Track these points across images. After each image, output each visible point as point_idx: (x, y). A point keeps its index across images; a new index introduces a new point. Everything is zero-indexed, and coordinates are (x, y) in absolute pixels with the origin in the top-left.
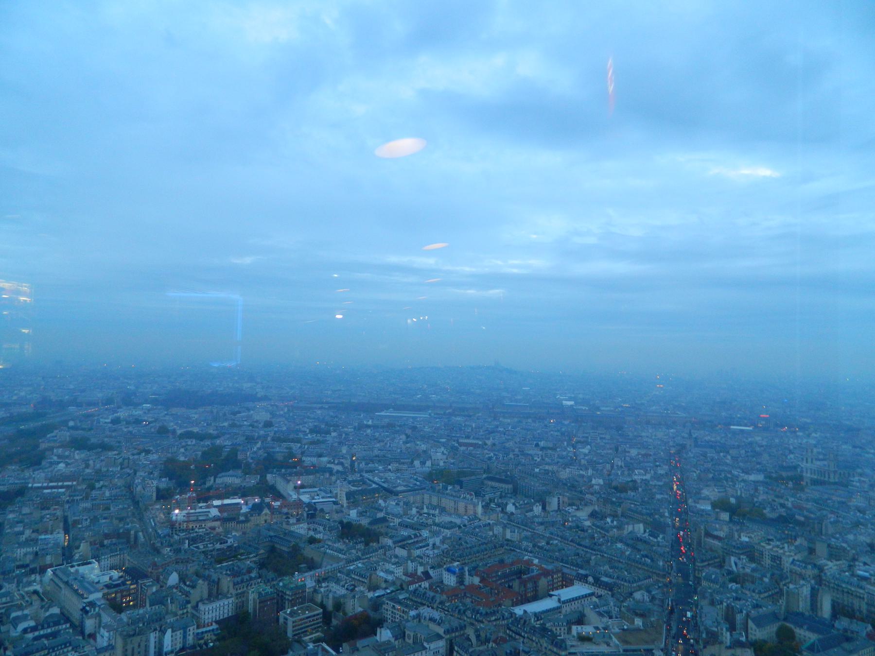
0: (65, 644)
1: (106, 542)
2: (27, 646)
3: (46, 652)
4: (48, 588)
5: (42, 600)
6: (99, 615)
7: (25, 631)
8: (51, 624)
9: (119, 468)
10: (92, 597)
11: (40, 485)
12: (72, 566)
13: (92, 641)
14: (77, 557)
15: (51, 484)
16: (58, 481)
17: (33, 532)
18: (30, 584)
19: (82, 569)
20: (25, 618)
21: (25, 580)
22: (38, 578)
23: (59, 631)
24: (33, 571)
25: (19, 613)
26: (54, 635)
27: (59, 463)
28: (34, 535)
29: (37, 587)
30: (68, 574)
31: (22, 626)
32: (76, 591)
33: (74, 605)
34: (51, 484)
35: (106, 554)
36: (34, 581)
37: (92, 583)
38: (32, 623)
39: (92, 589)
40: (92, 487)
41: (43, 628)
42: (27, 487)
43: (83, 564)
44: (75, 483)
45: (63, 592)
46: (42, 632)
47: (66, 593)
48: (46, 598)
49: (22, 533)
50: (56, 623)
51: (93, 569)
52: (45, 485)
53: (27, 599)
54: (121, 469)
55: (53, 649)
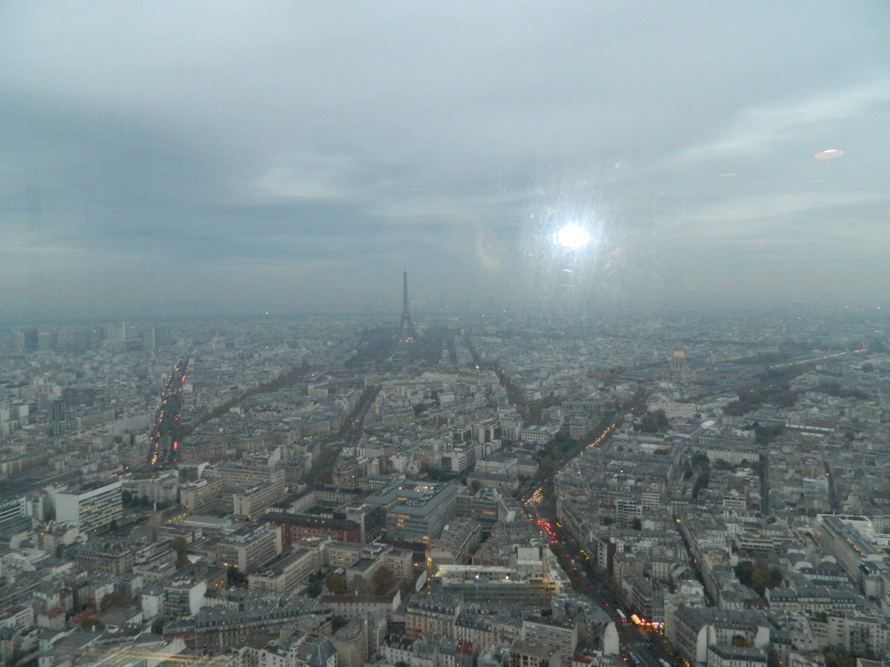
0: (849, 599)
1: (876, 500)
2: (809, 587)
3: (829, 600)
4: (819, 534)
5: (817, 544)
6: (881, 580)
7: (803, 570)
8: (829, 572)
9: (879, 421)
10: (871, 558)
11: (797, 426)
12: (843, 518)
13: (875, 605)
14: (846, 508)
15: (808, 427)
16: (815, 424)
17: (797, 472)
18: (802, 524)
19: (856, 524)
20: (801, 558)
21: (796, 519)
22: (807, 519)
23: (839, 582)
24: (802, 512)
25: (795, 551)
26: (835, 585)
27: (811, 407)
28: (797, 476)
29: (808, 529)
30: (841, 526)
31: (800, 565)
32: (852, 546)
33: (853, 562)
34: (808, 427)
35: (878, 513)
36: (806, 523)
37: (869, 542)
38: (810, 566)
39: (870, 550)
40: (852, 438)
41: (820, 574)
42: (783, 427)
43: (855, 519)
44: (832, 430)
45: (836, 541)
46: (820, 577)
47: (839, 545)
48: (821, 544)
49: (787, 472)
50: (834, 574)
51: (866, 526)
52: (802, 427)
53: (801, 538)
54: (883, 422)
55: (836, 600)
